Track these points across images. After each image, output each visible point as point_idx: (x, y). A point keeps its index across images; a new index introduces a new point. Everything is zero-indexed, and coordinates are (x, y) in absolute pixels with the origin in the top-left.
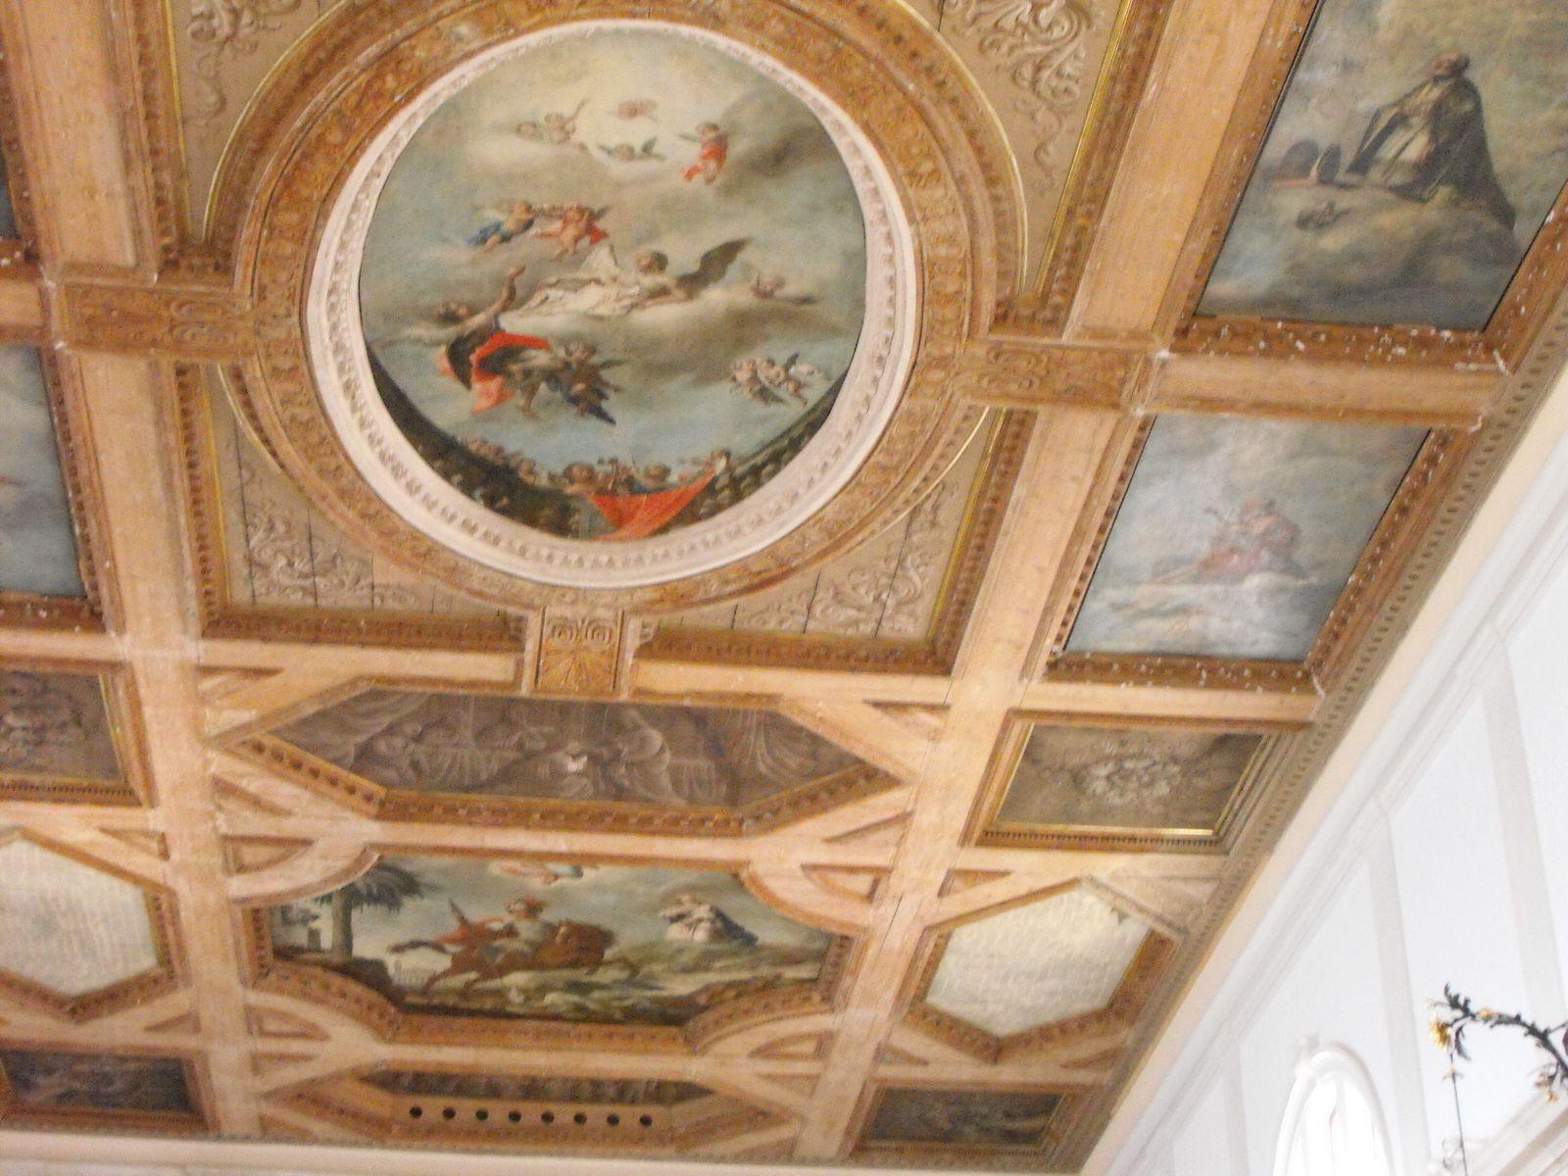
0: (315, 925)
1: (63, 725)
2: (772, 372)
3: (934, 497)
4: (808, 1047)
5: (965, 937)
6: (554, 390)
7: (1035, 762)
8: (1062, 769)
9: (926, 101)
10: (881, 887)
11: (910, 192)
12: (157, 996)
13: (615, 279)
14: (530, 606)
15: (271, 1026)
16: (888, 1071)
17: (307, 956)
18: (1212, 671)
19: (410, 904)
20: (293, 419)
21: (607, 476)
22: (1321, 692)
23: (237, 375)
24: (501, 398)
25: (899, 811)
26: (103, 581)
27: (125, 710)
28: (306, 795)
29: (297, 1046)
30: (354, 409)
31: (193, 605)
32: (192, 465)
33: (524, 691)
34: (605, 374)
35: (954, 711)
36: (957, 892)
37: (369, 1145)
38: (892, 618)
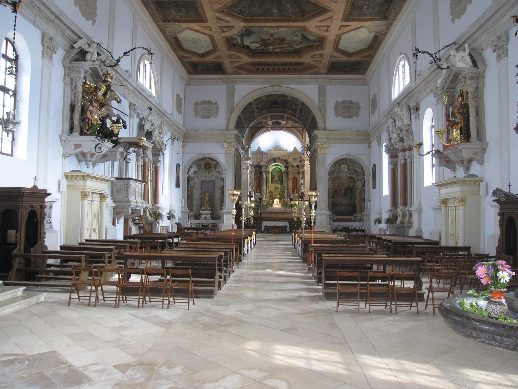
4: (319, 56)
5: (343, 37)
15: (232, 57)
16: (332, 59)
19: (252, 36)
27: (200, 6)
28: (232, 19)
29: (237, 60)
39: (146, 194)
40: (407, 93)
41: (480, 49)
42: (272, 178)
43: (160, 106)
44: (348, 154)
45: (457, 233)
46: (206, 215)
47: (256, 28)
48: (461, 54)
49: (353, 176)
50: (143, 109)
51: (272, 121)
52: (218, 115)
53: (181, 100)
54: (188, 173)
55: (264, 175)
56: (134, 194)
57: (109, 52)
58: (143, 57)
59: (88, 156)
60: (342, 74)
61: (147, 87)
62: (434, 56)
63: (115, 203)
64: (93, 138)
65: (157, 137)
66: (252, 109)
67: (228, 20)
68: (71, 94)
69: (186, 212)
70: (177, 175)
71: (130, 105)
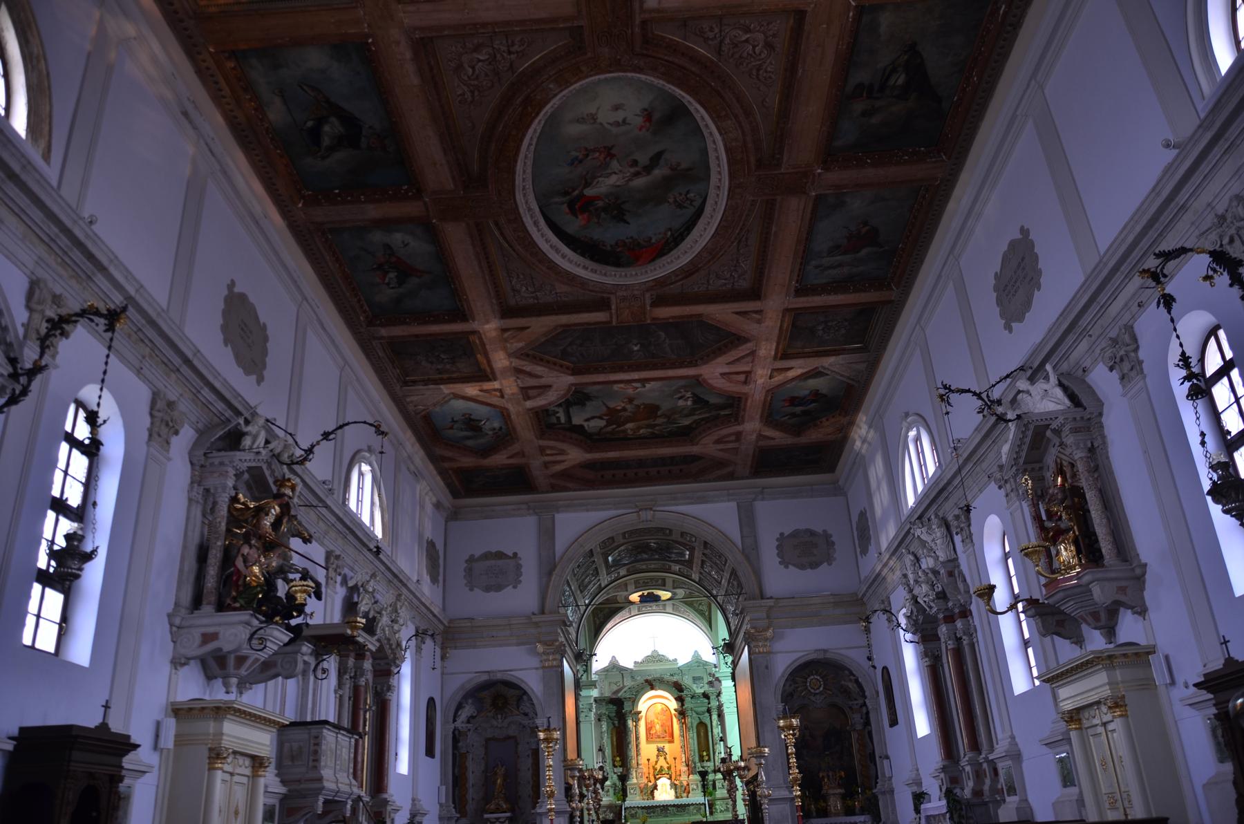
0: (558, 415)
2: (681, 198)
9: (719, 88)
10: (749, 378)
11: (719, 124)
13: (621, 171)
14: (612, 293)
15: (548, 452)
16: (761, 443)
19: (588, 403)
22: (895, 289)
23: (497, 224)
28: (546, 370)
29: (559, 458)
30: (539, 231)
32: (487, 258)
33: (614, 324)
37: (589, 490)
40: (937, 490)
41: (1081, 370)
42: (648, 729)
44: (819, 650)
45: (1123, 789)
48: (1041, 385)
50: (356, 568)
51: (640, 593)
53: (437, 552)
54: (454, 721)
55: (630, 723)
57: (290, 434)
58: (357, 457)
59: (231, 661)
60: (784, 475)
61: (366, 519)
62: (984, 396)
63: (284, 786)
64: (245, 616)
65: (387, 629)
66: (594, 566)
67: (540, 374)
68: (203, 522)
69: (450, 819)
71: (329, 555)
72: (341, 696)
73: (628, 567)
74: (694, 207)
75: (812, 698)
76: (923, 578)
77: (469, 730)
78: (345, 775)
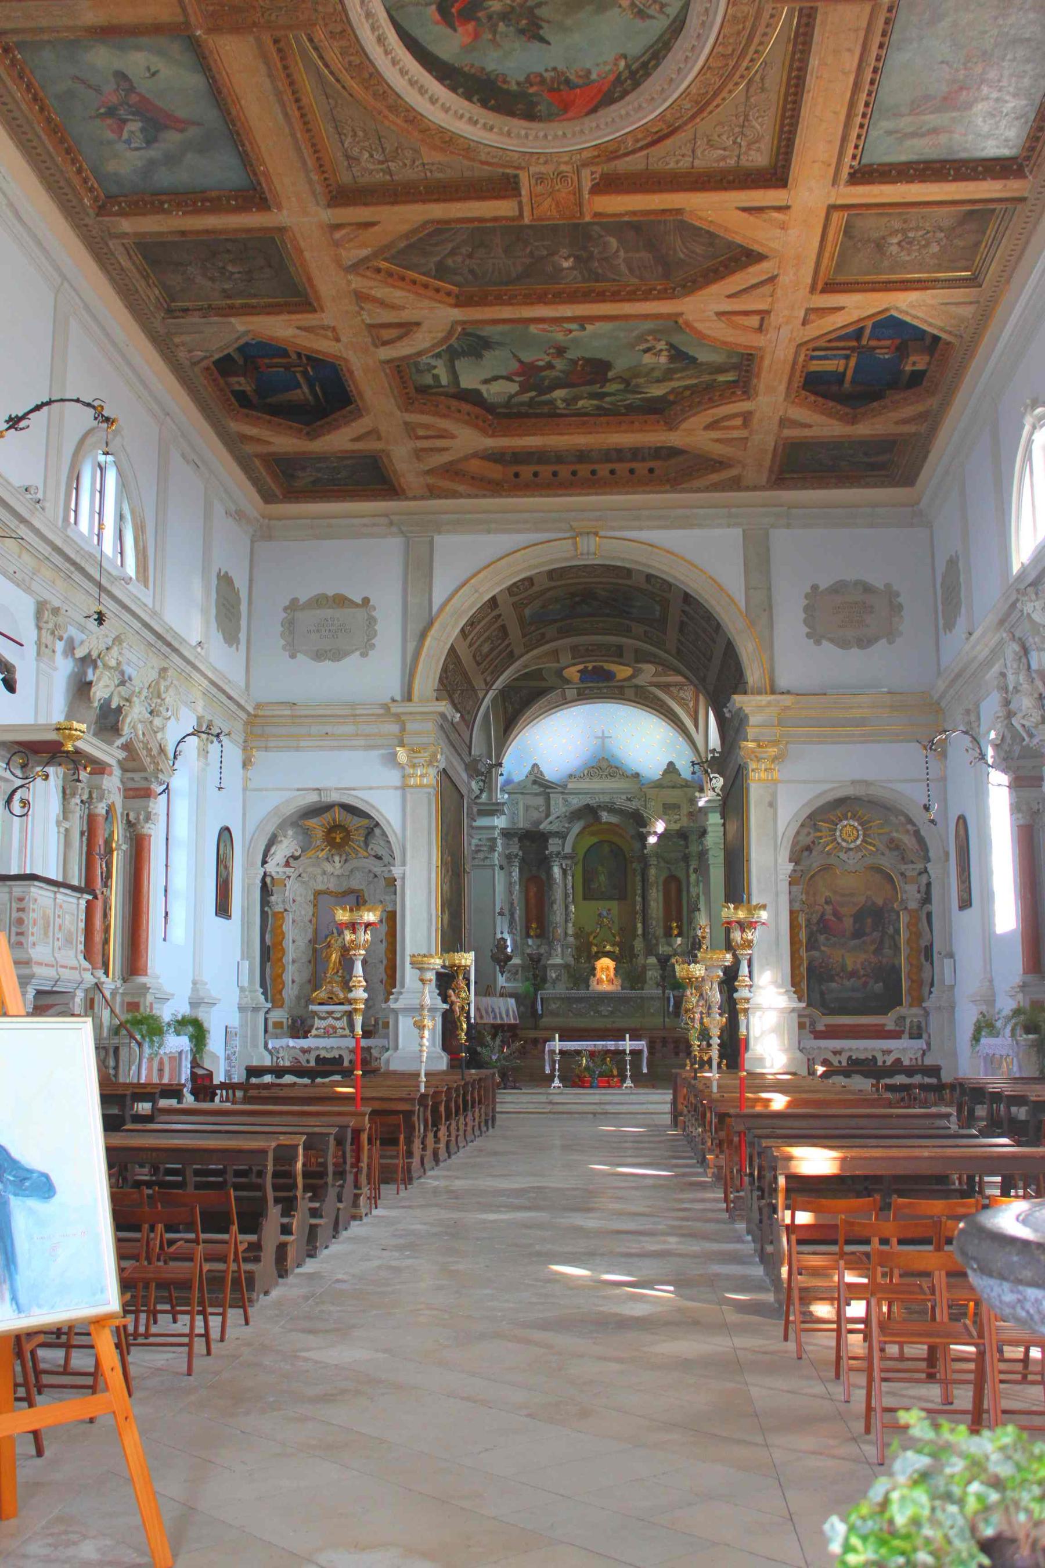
0: (435, 372)
1: (262, 268)
3: (761, 71)
4: (738, 422)
6: (508, 26)
7: (851, 238)
8: (869, 240)
10: (766, 322)
12: (352, 421)
15: (421, 432)
16: (787, 432)
17: (434, 390)
18: (957, 170)
19: (487, 354)
20: (350, 63)
21: (553, 80)
22: (1030, 177)
23: (311, 40)
24: (476, 36)
25: (770, 275)
26: (262, 180)
28: (412, 296)
29: (440, 443)
30: (387, 53)
31: (319, 189)
32: (297, 100)
33: (527, 221)
34: (537, 12)
35: (793, 210)
36: (813, 322)
38: (746, 153)
39: (98, 938)
43: (155, 613)
46: (330, 1021)
47: (500, 328)
49: (887, 862)
52: (373, 646)
53: (238, 594)
54: (264, 862)
55: (556, 871)
56: (46, 934)
60: (827, 486)
65: (140, 726)
66: (500, 622)
67: (396, 301)
69: (256, 1009)
70: (222, 868)
72: (67, 830)
73: (559, 624)
74: (668, 16)
75: (842, 855)
76: (1025, 686)
77: (289, 877)
78: (72, 953)
